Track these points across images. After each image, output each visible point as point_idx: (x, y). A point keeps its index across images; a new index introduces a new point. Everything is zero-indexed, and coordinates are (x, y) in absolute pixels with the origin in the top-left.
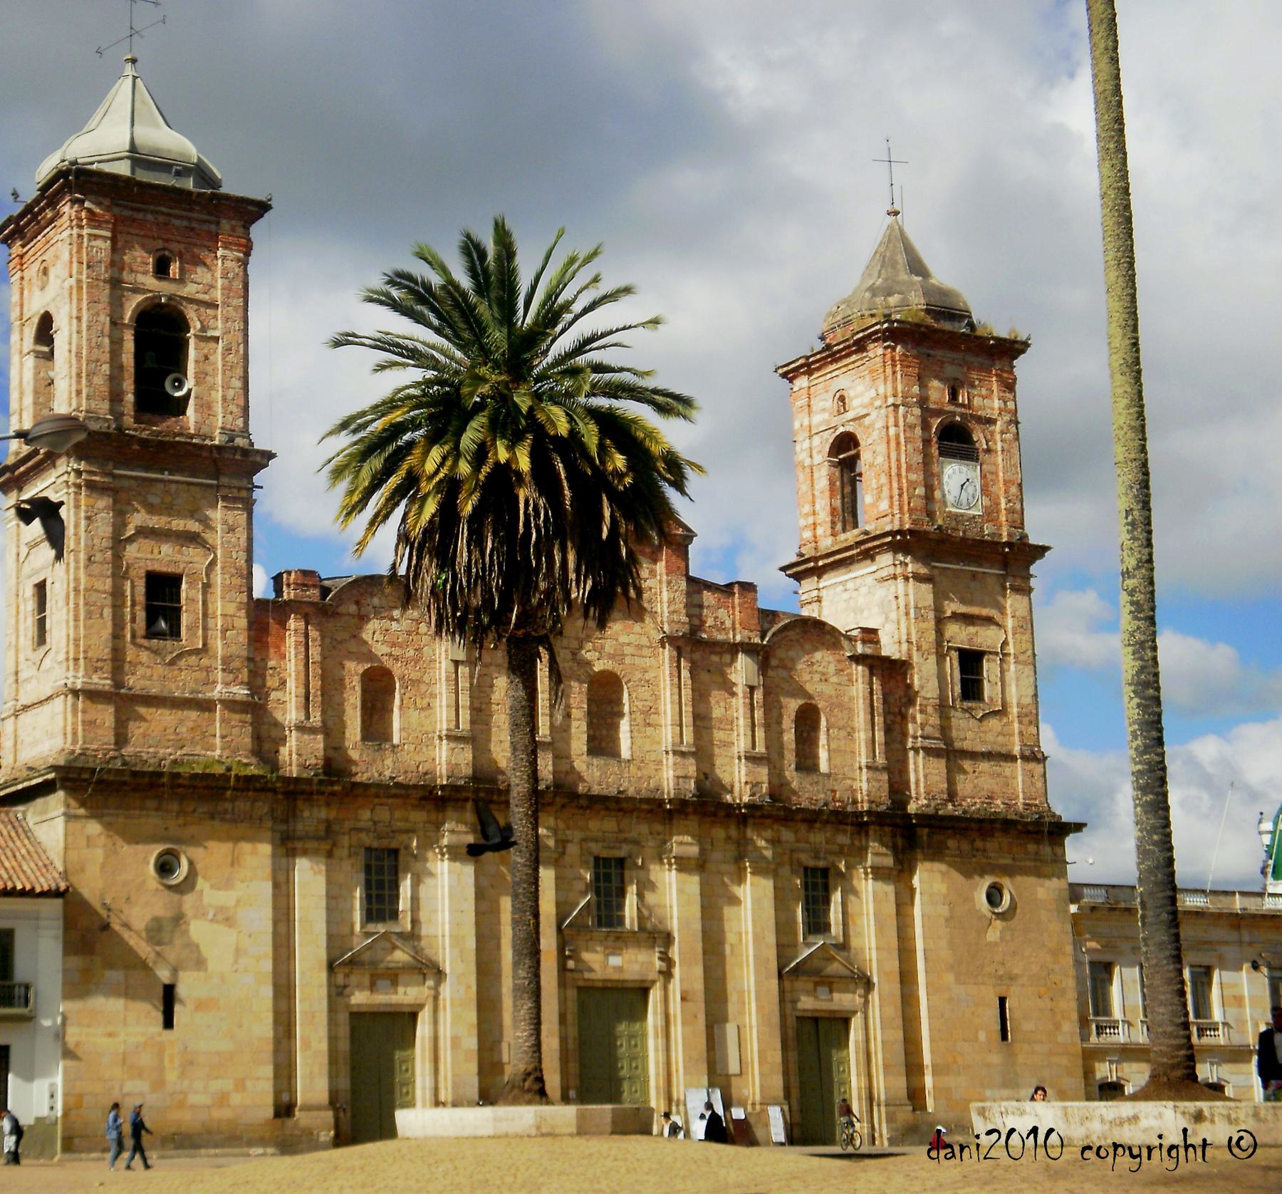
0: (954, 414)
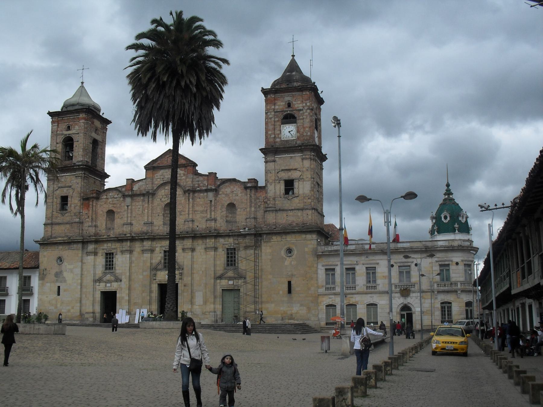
0: (287, 111)
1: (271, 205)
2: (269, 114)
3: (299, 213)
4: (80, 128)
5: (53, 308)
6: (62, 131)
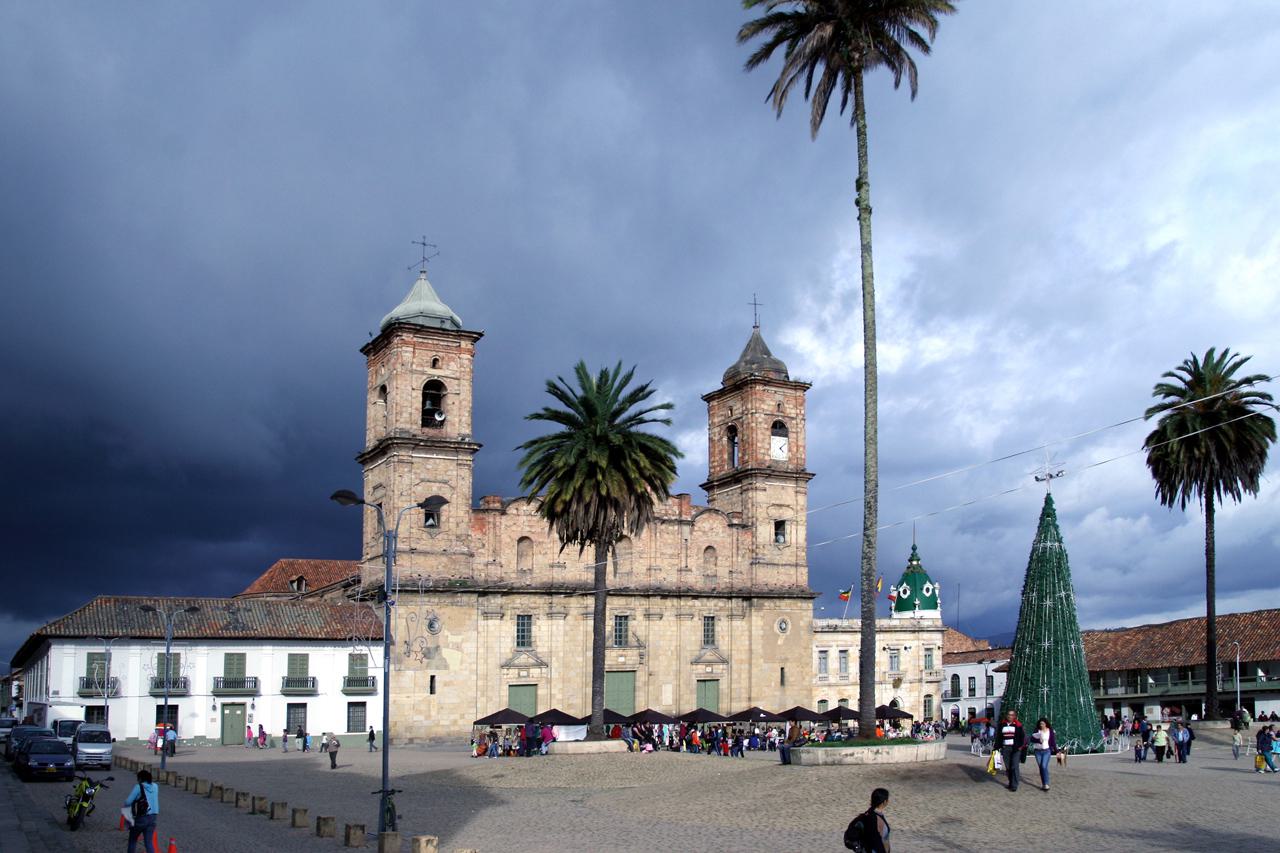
0: (778, 416)
1: (760, 556)
2: (757, 415)
3: (792, 571)
4: (463, 369)
5: (421, 718)
6: (422, 366)
